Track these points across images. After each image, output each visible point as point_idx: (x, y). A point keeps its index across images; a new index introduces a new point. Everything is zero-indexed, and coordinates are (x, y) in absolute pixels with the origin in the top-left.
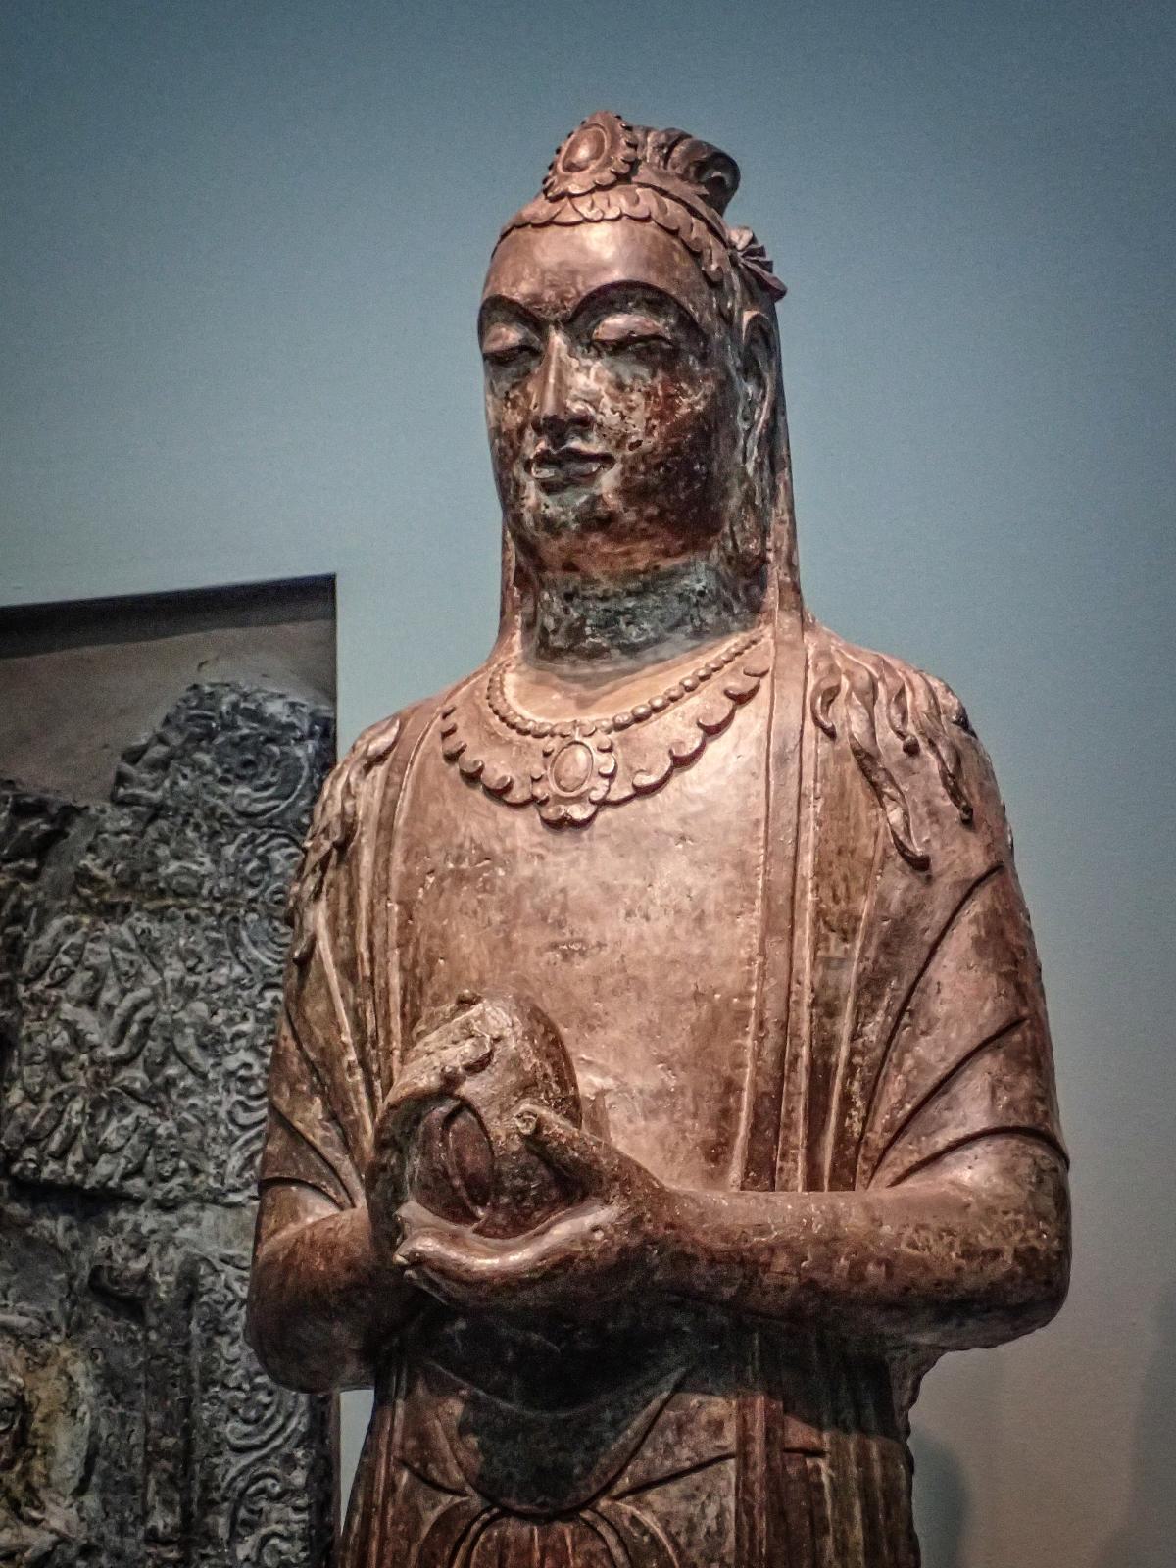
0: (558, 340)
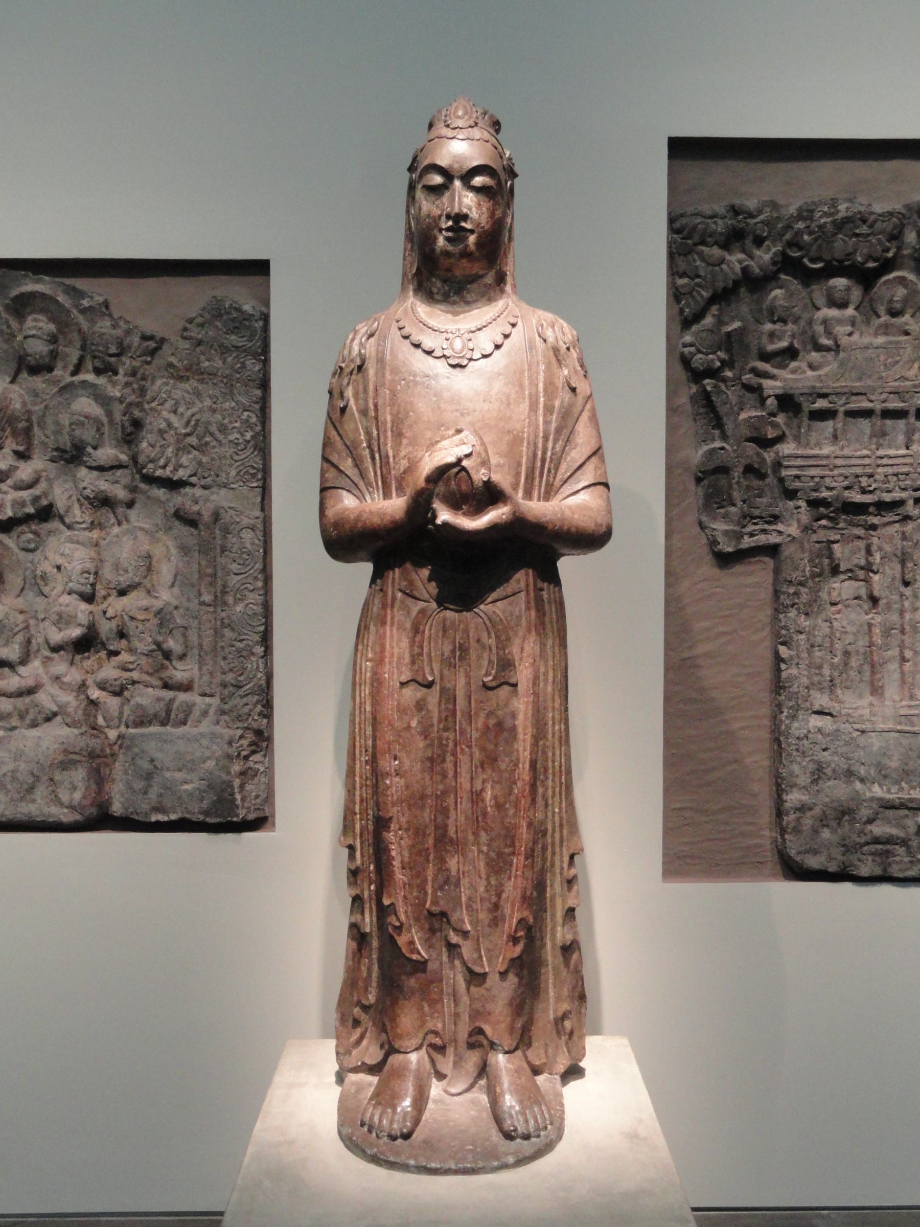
0: (457, 183)
